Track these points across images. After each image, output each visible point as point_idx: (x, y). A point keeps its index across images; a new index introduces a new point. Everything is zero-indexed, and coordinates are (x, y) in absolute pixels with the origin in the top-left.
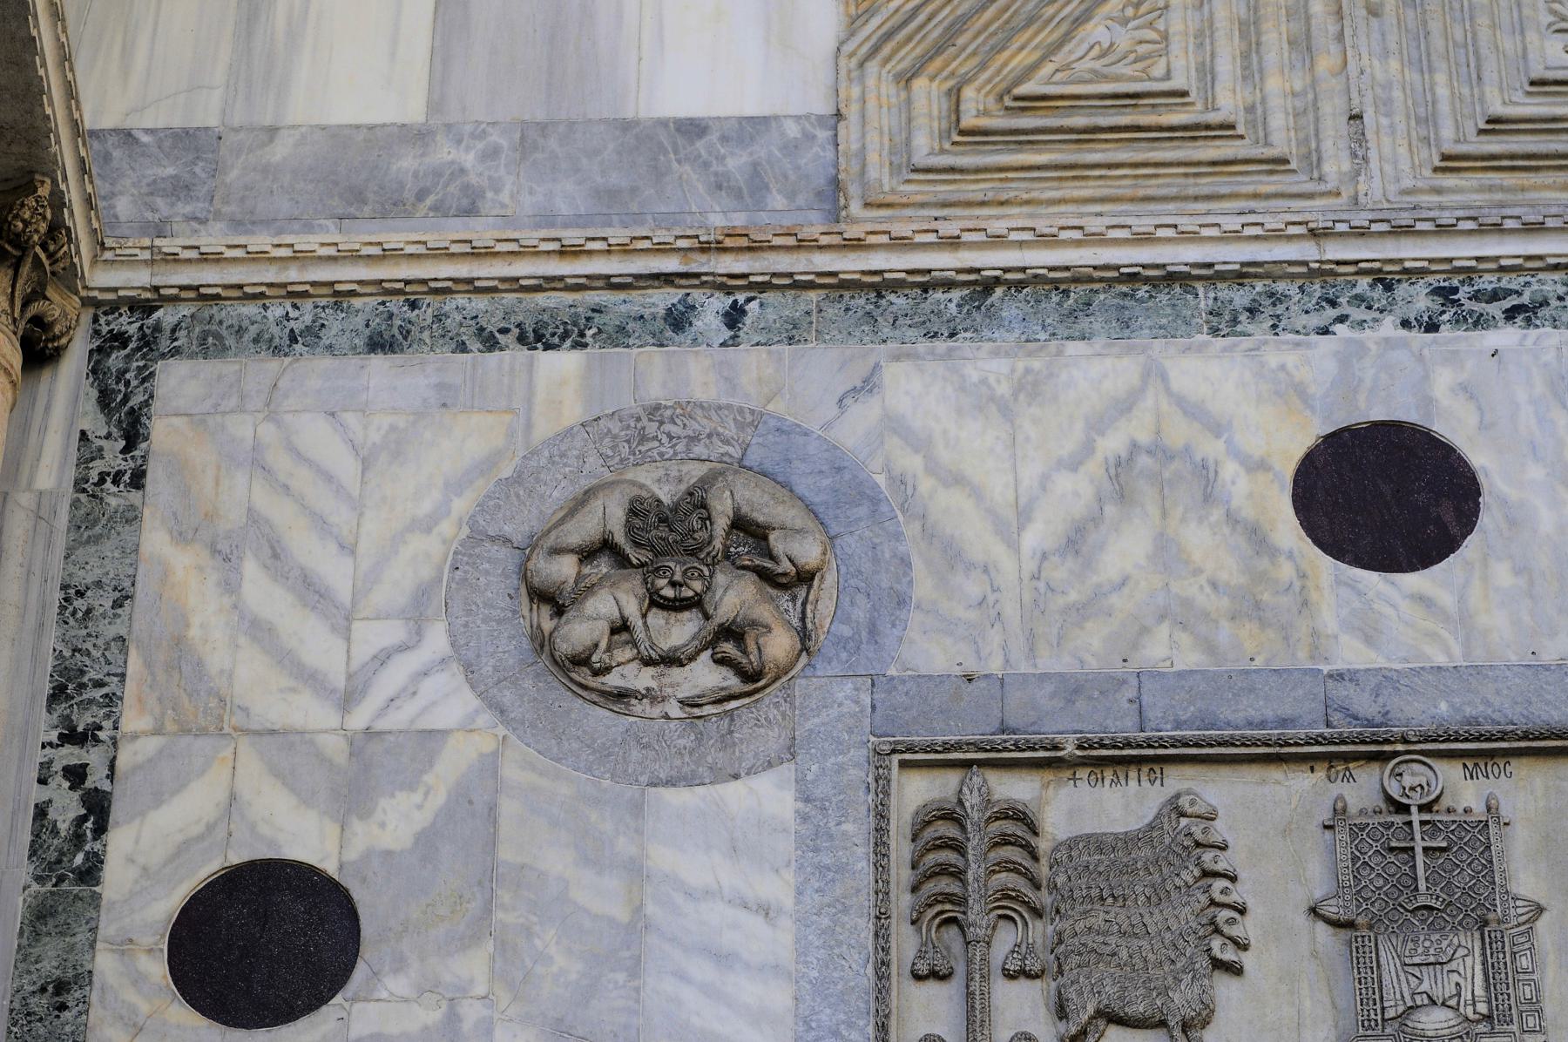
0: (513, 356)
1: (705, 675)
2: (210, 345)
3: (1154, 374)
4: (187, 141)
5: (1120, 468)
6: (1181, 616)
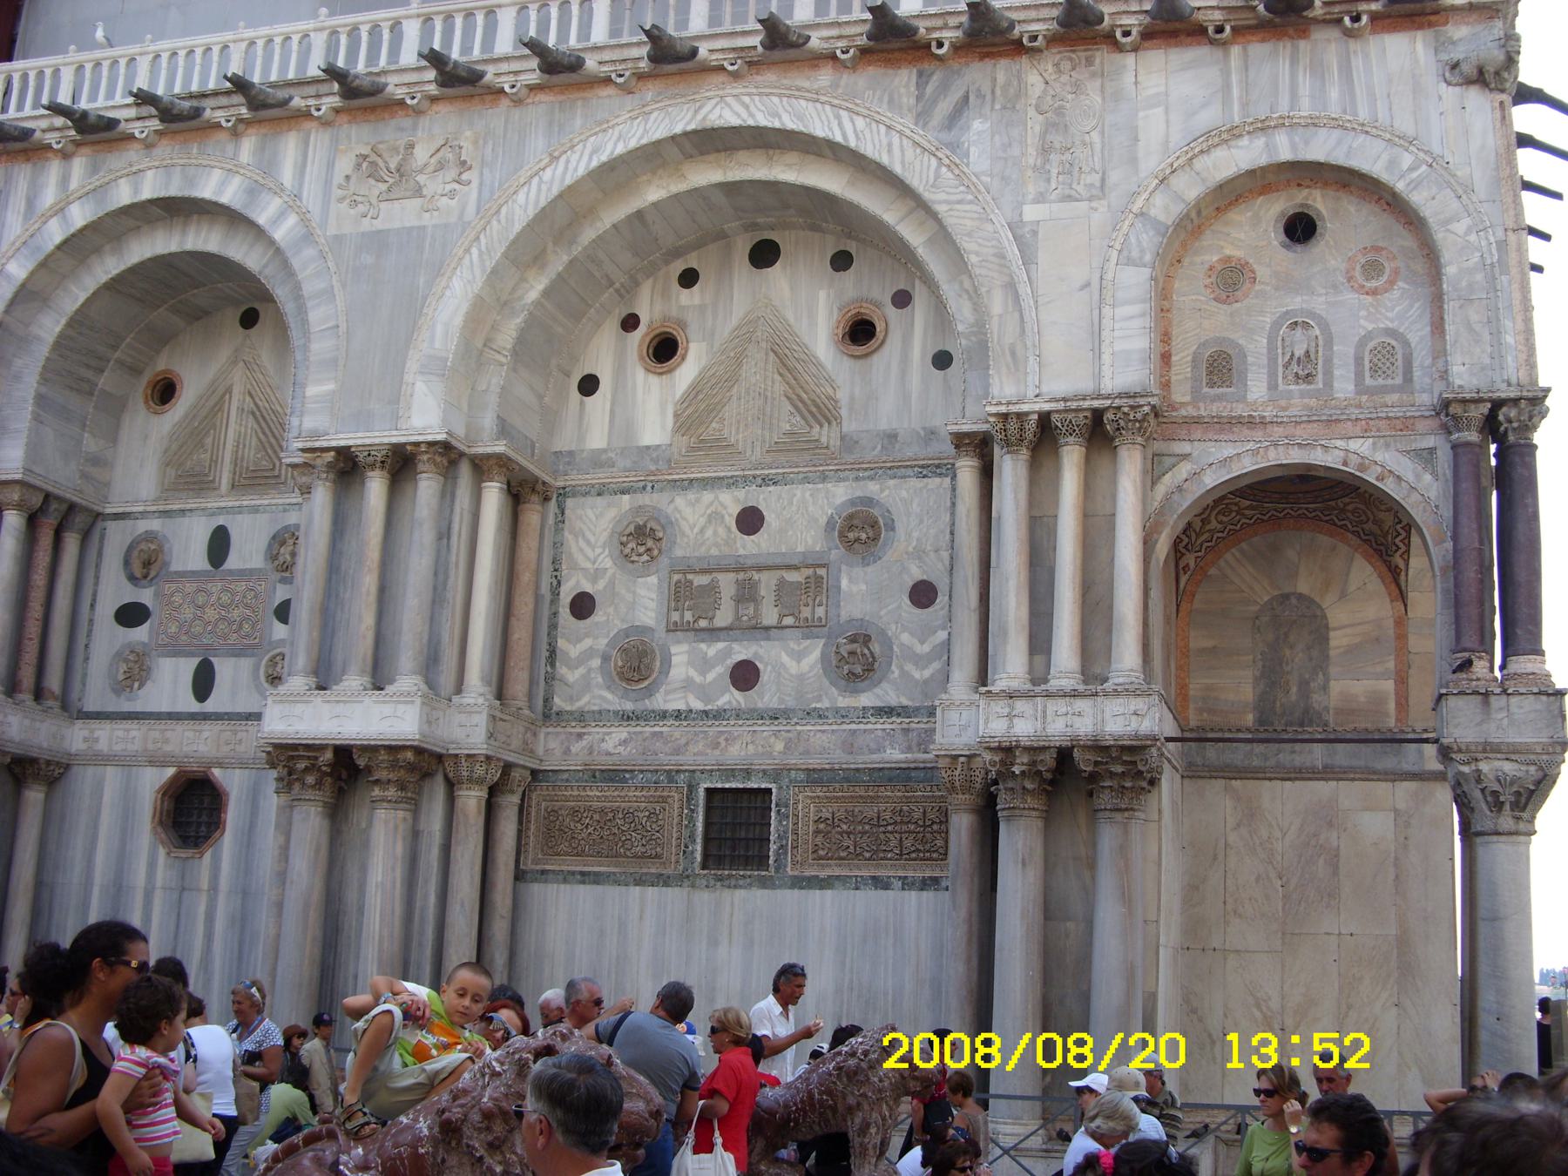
0: (619, 496)
1: (645, 558)
2: (574, 495)
3: (717, 497)
4: (571, 453)
5: (710, 515)
6: (716, 545)
